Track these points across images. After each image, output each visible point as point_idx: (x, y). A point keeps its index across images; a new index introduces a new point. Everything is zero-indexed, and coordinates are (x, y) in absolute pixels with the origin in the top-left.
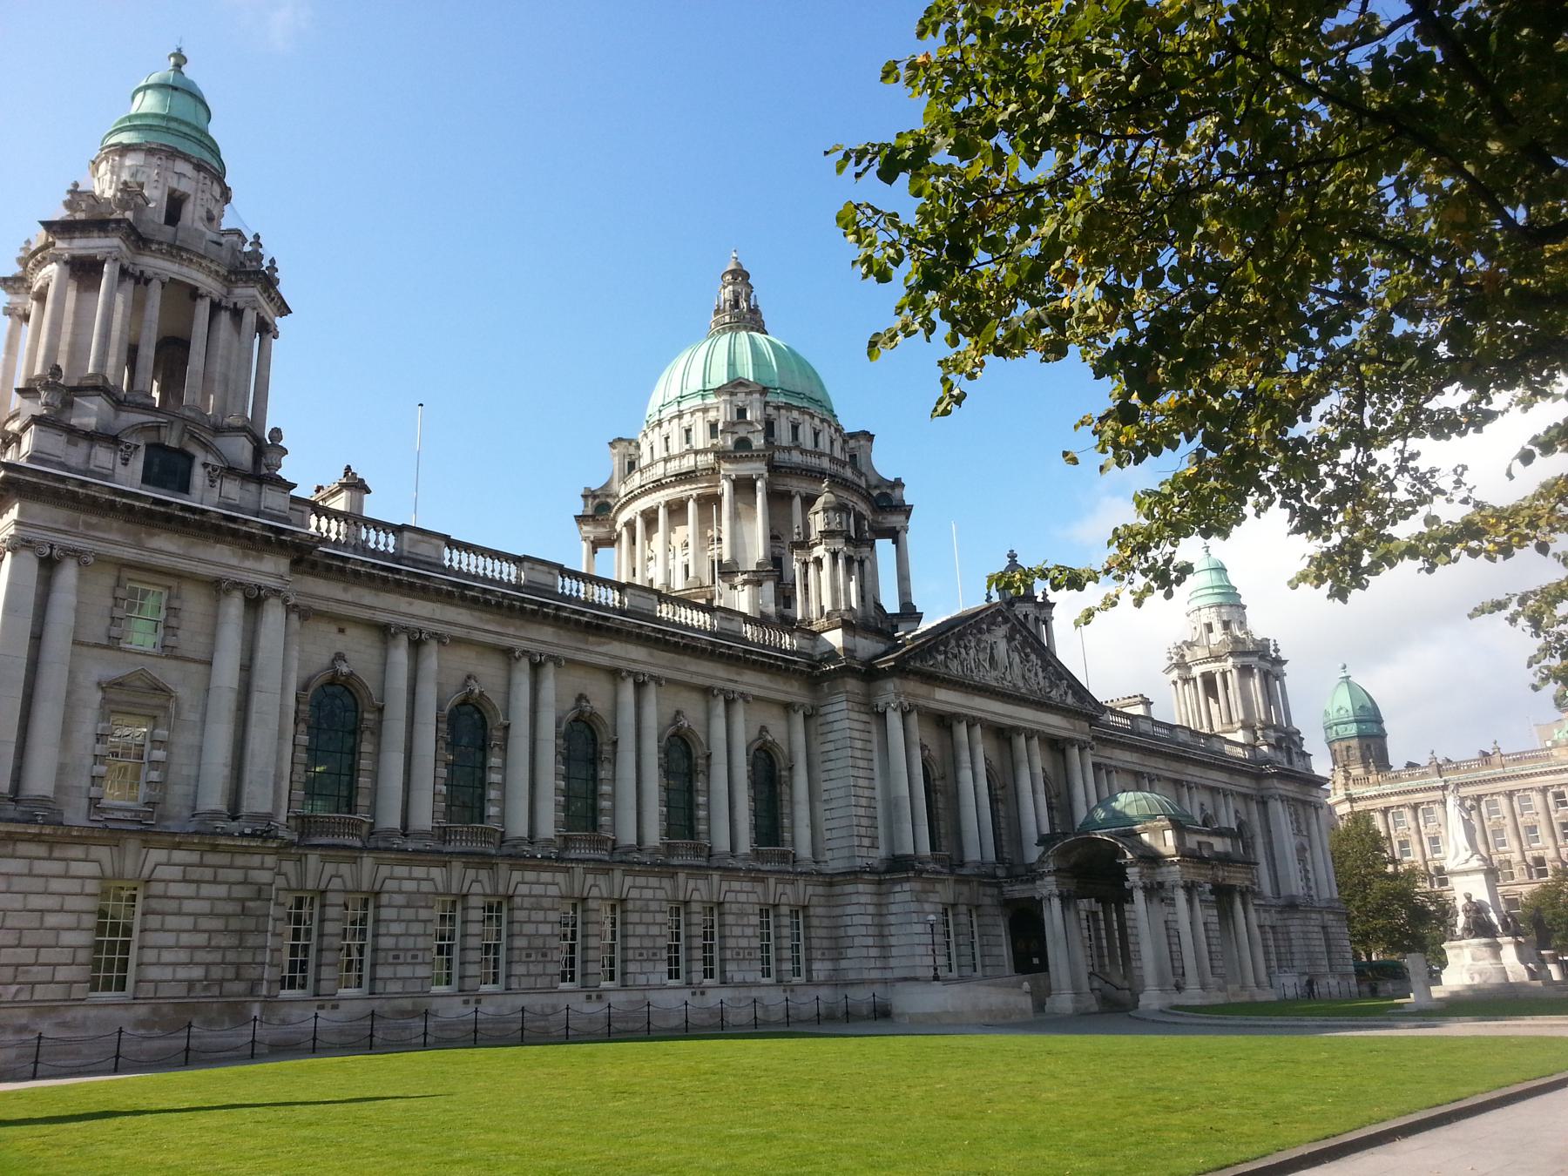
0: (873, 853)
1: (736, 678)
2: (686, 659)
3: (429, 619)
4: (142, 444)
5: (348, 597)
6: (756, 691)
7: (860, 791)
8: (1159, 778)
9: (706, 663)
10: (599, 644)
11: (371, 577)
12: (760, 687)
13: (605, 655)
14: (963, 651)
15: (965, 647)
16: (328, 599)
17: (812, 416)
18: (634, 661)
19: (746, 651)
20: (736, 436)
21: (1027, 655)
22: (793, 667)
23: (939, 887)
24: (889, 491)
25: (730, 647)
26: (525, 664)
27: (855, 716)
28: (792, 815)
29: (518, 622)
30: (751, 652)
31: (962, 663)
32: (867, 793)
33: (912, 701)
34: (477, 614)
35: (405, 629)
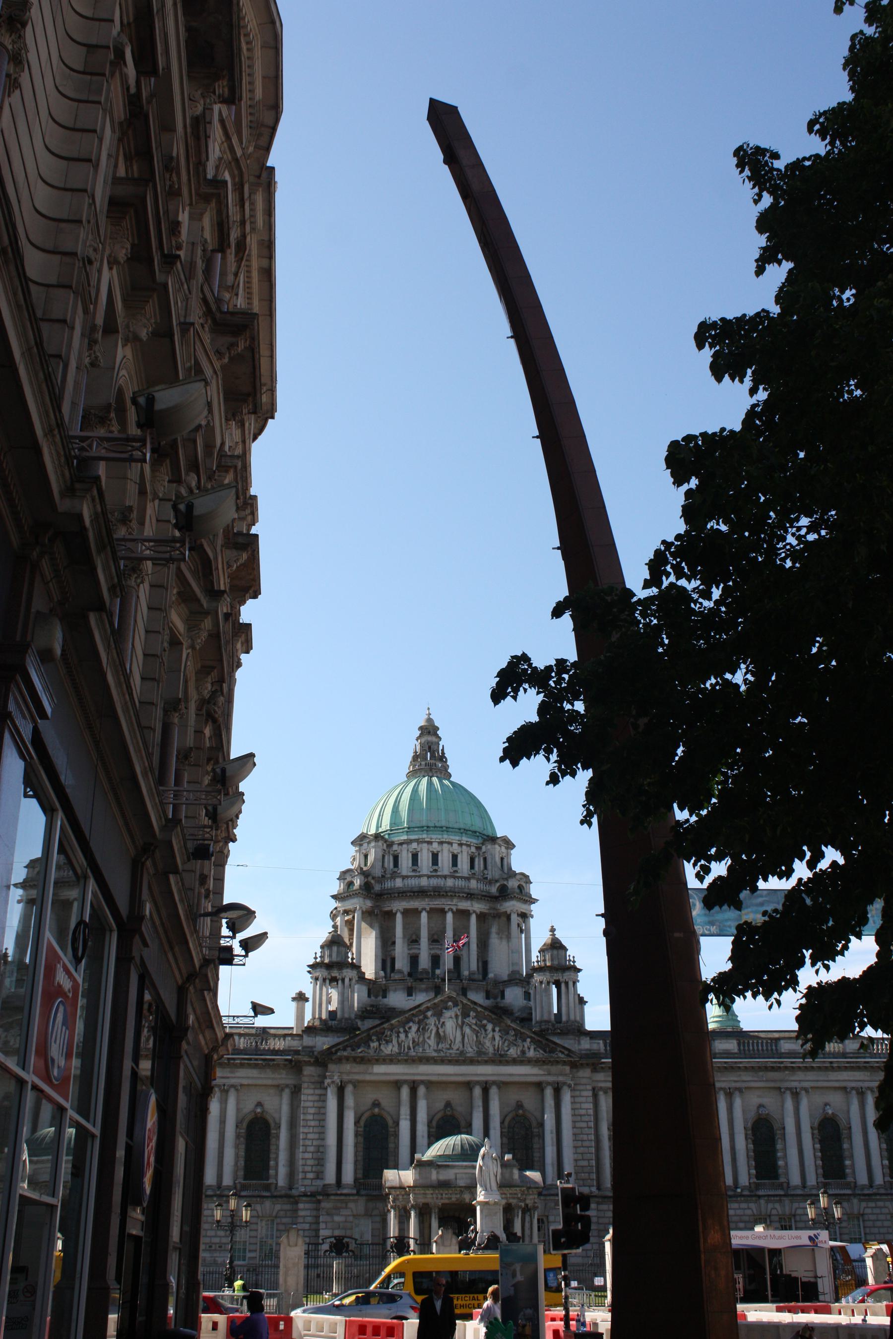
0: (319, 1183)
1: (229, 1075)
6: (245, 1082)
7: (309, 1143)
8: (740, 1090)
12: (248, 1078)
14: (402, 1036)
15: (406, 1032)
17: (430, 843)
20: (346, 881)
21: (484, 1026)
22: (271, 1063)
23: (351, 1205)
24: (505, 883)
27: (310, 1091)
28: (276, 1160)
30: (234, 1059)
31: (399, 1045)
32: (315, 1143)
33: (345, 1078)
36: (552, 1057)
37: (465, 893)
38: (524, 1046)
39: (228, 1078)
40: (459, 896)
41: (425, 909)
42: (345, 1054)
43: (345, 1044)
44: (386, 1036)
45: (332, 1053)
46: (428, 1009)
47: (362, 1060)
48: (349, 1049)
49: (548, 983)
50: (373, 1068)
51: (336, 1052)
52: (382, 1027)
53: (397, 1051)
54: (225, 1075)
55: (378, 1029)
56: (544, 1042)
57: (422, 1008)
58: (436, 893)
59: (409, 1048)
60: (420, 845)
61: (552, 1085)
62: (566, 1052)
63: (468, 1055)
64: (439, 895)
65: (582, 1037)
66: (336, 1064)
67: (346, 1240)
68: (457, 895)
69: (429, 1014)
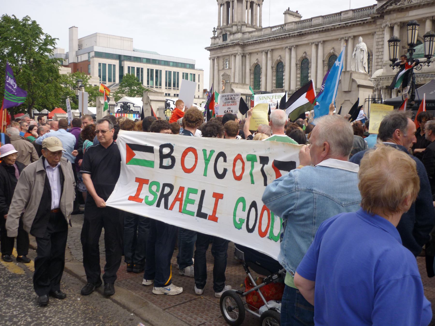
2: (331, 32)
3: (268, 47)
4: (221, 36)
5: (254, 48)
9: (337, 31)
10: (305, 38)
11: (254, 43)
13: (306, 40)
16: (251, 50)
18: (314, 39)
19: (346, 24)
22: (366, 22)
25: (339, 25)
26: (287, 50)
29: (285, 40)
30: (348, 23)
33: (394, 22)
34: (277, 42)
35: (263, 51)
39: (347, 33)
42: (391, 7)
43: (391, 2)
45: (384, 9)
47: (401, 10)
48: (394, 5)
51: (387, 7)
54: (346, 33)
66: (388, 15)
67: (129, 104)
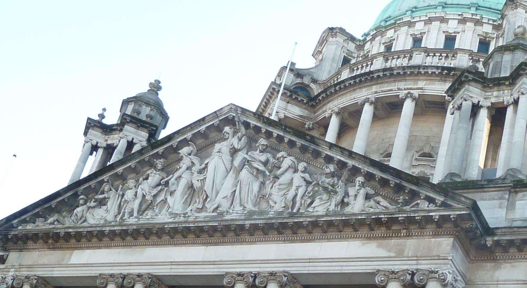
14: (129, 194)
36: (401, 211)
37: (437, 68)
38: (347, 194)
40: (426, 73)
41: (367, 100)
44: (103, 193)
46: (185, 143)
49: (476, 109)
50: (71, 254)
52: (100, 179)
53: (110, 217)
55: (93, 183)
56: (393, 181)
57: (174, 143)
58: (388, 73)
59: (131, 214)
60: (398, 32)
61: (397, 279)
62: (440, 199)
63: (228, 217)
64: (392, 75)
65: (520, 195)
68: (422, 71)
69: (185, 151)
